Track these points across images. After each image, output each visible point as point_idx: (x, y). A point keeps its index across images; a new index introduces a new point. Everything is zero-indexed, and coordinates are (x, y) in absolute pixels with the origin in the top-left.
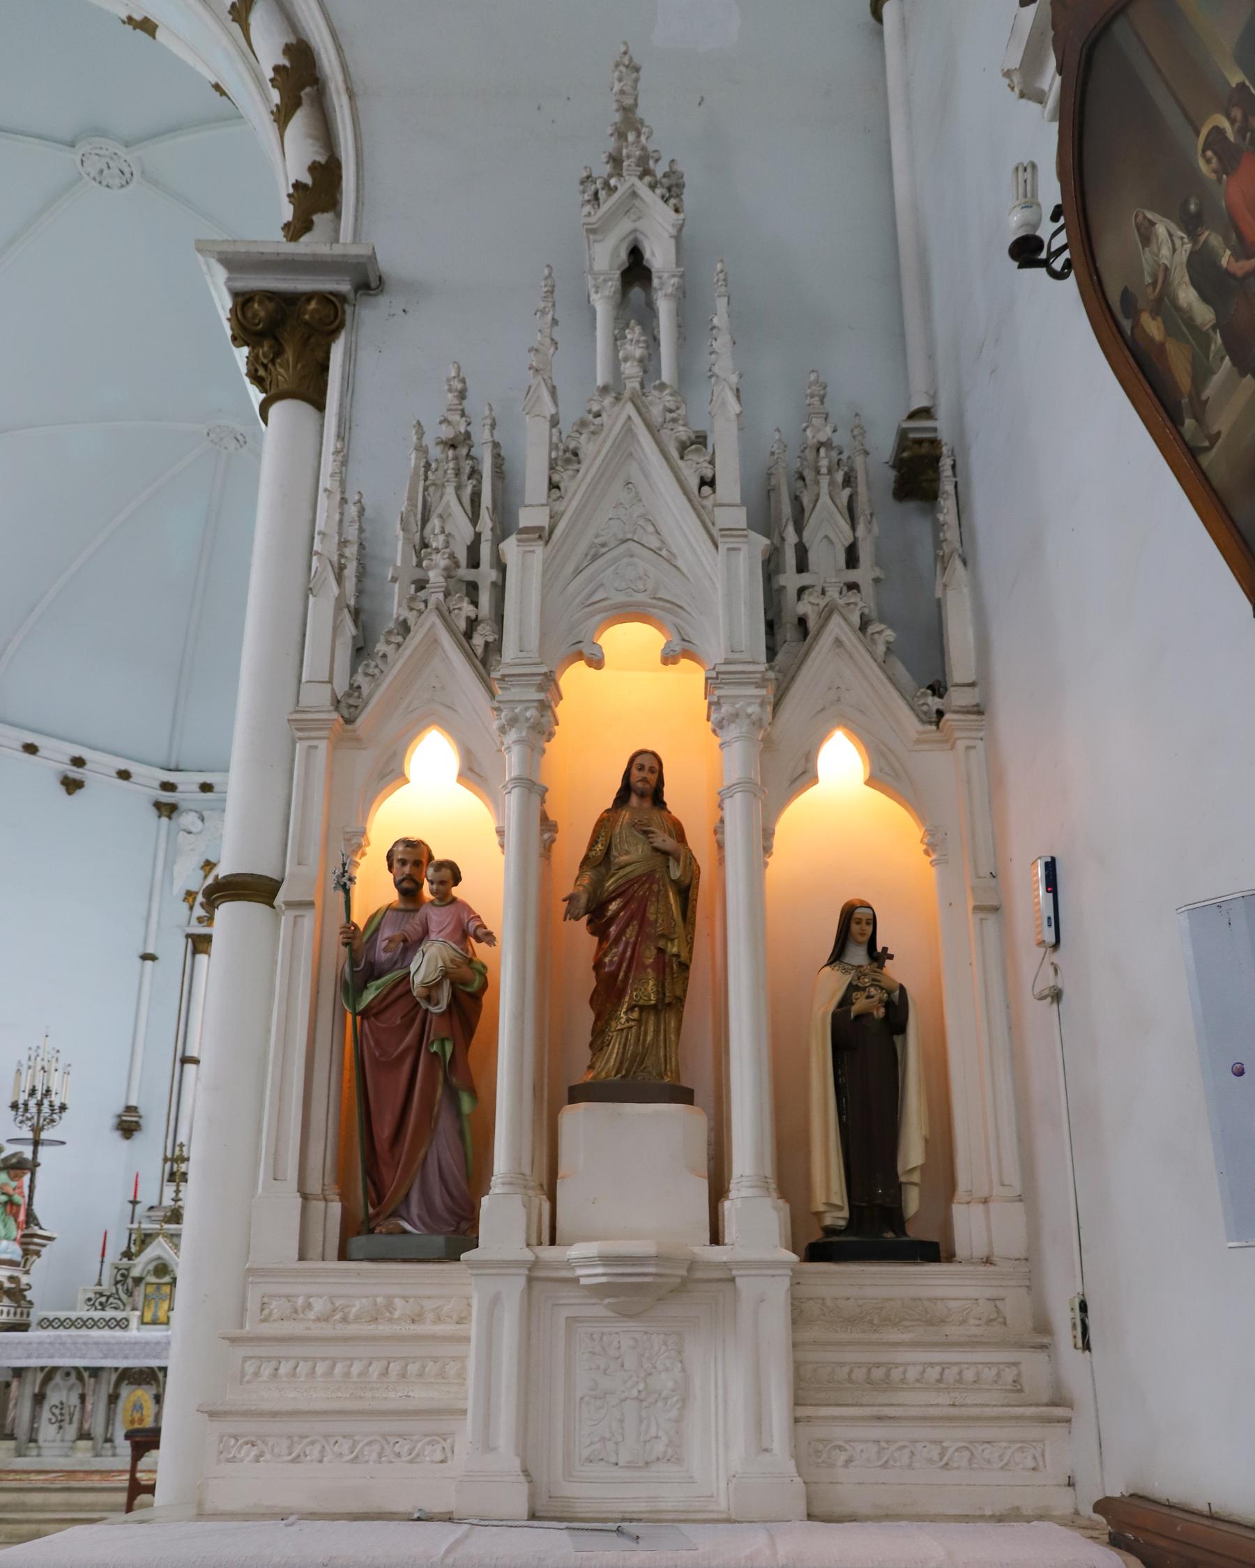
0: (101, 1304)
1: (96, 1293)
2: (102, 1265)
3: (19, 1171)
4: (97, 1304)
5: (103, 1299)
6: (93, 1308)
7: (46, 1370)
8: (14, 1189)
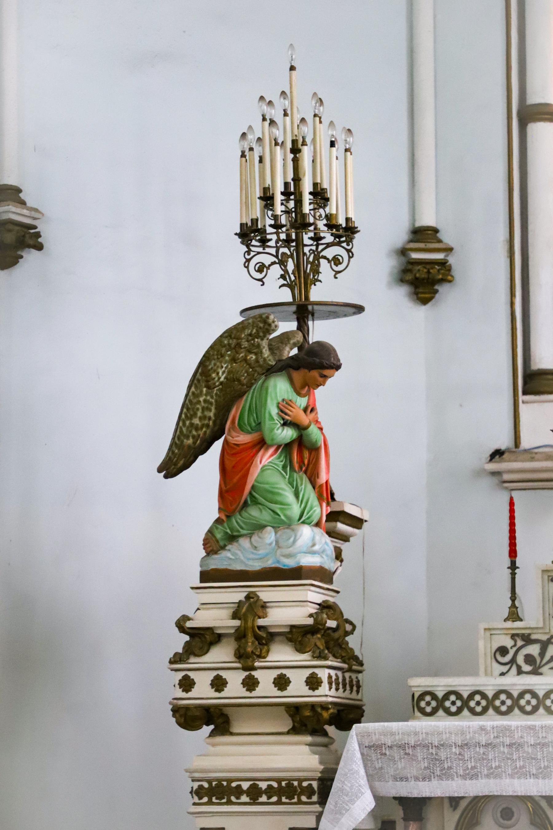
0: (529, 659)
1: (513, 636)
2: (513, 575)
3: (315, 373)
4: (520, 659)
5: (534, 650)
6: (514, 669)
7: (463, 804)
8: (305, 410)
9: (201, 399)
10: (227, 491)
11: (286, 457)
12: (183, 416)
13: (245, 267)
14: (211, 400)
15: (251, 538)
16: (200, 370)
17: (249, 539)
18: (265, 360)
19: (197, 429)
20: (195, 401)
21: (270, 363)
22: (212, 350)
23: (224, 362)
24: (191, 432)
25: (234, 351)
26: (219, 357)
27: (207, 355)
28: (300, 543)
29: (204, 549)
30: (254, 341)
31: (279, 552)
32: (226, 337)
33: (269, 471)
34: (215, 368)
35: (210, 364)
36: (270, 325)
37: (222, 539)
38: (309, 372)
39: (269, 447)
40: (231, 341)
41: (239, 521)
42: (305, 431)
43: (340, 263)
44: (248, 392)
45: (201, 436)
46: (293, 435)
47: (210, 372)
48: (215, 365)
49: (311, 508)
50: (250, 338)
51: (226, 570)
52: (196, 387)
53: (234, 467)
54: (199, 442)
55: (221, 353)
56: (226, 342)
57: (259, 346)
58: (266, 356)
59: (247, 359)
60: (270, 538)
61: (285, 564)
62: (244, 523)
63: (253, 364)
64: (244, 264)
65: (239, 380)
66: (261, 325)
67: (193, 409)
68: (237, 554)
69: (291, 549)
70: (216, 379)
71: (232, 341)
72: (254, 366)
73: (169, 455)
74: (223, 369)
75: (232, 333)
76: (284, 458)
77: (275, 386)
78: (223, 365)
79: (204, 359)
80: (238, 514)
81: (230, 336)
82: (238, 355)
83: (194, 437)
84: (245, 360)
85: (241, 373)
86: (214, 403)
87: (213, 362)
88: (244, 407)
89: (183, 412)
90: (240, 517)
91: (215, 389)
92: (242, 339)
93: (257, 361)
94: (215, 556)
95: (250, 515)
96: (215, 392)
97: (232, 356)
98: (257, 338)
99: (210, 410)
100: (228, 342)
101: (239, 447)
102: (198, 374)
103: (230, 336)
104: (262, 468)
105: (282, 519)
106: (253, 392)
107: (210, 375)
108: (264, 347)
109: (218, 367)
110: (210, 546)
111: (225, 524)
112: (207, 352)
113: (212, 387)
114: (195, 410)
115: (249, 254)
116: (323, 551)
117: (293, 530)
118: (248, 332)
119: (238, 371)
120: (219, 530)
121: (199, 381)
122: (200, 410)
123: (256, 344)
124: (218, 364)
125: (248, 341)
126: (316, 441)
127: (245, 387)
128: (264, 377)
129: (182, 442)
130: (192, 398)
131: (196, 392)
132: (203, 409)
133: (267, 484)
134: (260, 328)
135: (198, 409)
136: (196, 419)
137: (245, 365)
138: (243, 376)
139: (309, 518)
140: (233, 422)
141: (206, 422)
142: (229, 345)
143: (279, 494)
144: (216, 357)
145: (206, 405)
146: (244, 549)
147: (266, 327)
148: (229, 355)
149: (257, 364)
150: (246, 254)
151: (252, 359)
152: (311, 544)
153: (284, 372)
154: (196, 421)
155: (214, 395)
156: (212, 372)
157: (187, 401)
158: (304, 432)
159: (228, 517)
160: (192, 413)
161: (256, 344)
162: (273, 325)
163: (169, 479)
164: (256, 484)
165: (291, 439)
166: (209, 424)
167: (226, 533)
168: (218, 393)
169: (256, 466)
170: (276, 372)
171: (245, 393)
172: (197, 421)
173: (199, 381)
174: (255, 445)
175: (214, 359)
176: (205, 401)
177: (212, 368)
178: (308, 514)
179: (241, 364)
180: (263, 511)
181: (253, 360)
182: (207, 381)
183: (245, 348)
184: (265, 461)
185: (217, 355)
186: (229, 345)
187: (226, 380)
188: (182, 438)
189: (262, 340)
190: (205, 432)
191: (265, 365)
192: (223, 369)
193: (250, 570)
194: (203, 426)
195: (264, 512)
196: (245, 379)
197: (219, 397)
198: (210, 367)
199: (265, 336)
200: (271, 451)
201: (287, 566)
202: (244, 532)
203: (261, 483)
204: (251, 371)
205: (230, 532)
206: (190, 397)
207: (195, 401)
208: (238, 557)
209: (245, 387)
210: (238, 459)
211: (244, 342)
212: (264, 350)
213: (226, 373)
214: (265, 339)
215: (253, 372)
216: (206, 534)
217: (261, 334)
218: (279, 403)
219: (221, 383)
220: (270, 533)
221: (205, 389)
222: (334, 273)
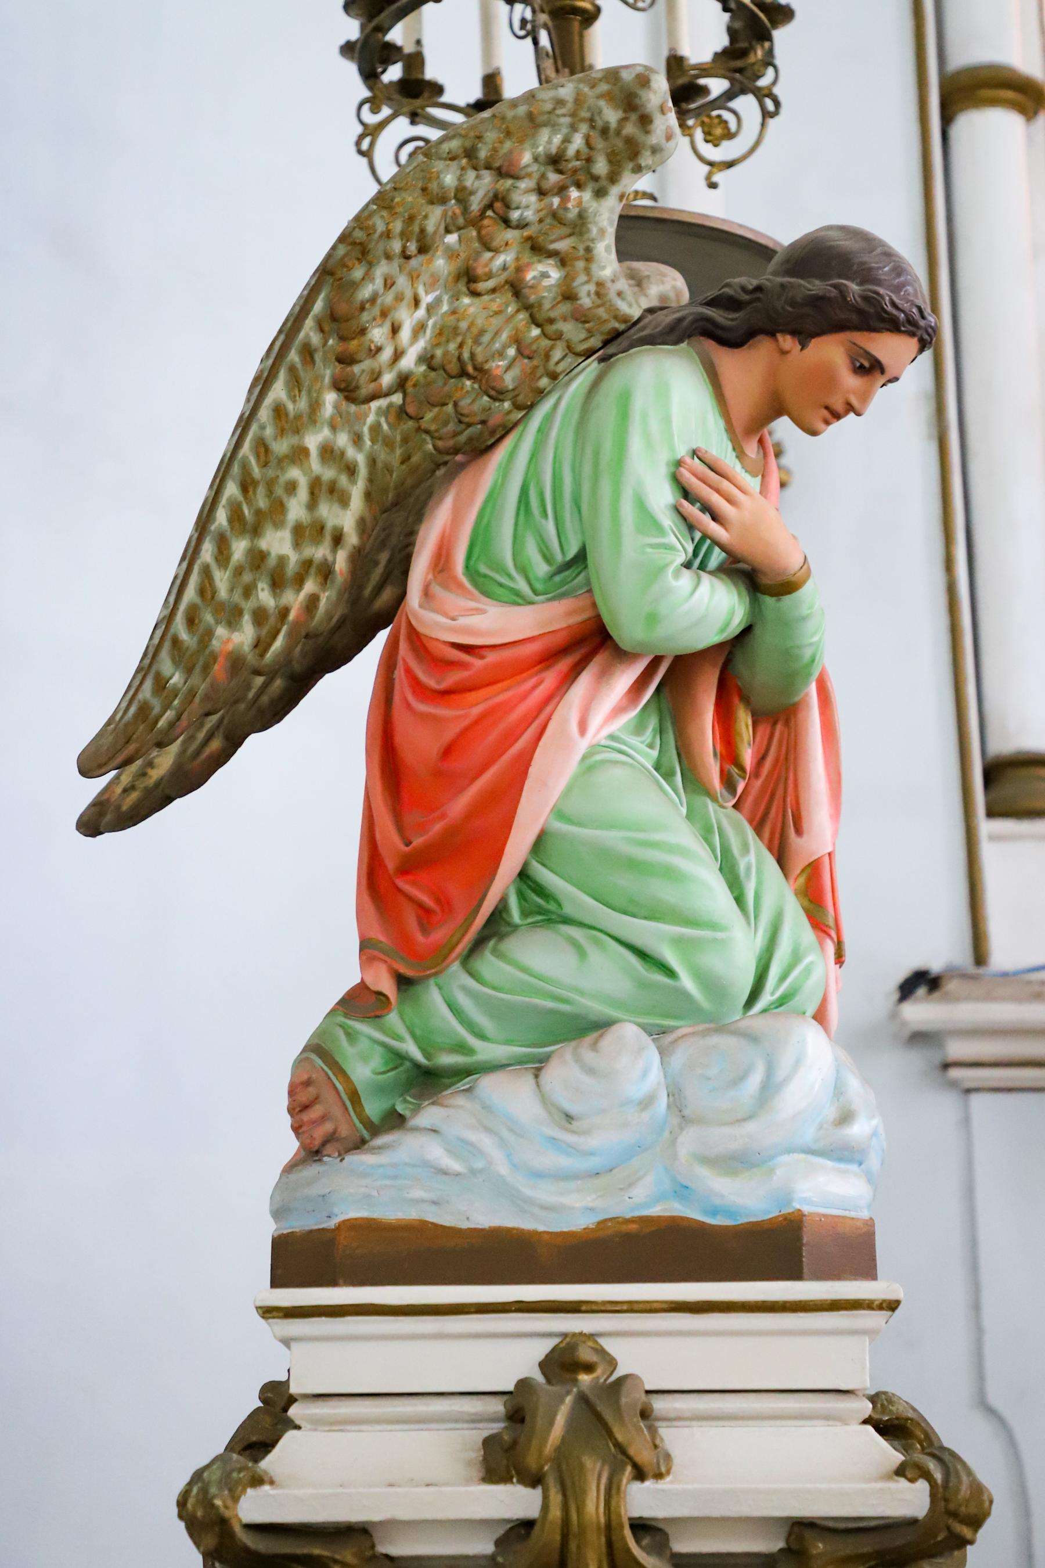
9: (313, 441)
10: (409, 866)
11: (662, 731)
12: (221, 517)
13: (361, 152)
14: (351, 453)
15: (537, 1076)
16: (318, 306)
17: (530, 1078)
19: (277, 584)
22: (385, 213)
23: (425, 277)
25: (474, 233)
26: (412, 247)
27: (359, 235)
29: (297, 1129)
30: (565, 200)
31: (688, 1141)
33: (617, 772)
34: (388, 298)
35: (367, 277)
36: (645, 121)
37: (381, 1090)
38: (803, 346)
39: (622, 655)
41: (464, 1002)
42: (787, 599)
43: (729, 135)
44: (520, 428)
45: (292, 616)
47: (365, 316)
48: (389, 283)
49: (796, 958)
50: (553, 178)
51: (421, 1229)
52: (295, 383)
53: (448, 751)
54: (279, 643)
55: (422, 231)
56: (449, 179)
57: (579, 226)
60: (645, 1074)
61: (717, 1201)
62: (497, 1011)
63: (547, 305)
64: (358, 143)
65: (480, 373)
66: (611, 116)
67: (270, 485)
68: (475, 1150)
69: (751, 1127)
70: (387, 354)
71: (478, 177)
72: (553, 314)
73: (140, 696)
74: (421, 312)
75: (479, 138)
76: (654, 736)
77: (663, 391)
78: (421, 291)
79: (342, 250)
80: (456, 967)
81: (470, 153)
82: (488, 255)
84: (516, 288)
85: (493, 340)
86: (363, 471)
87: (382, 270)
88: (493, 498)
89: (224, 501)
90: (470, 982)
91: (374, 405)
94: (356, 1160)
95: (524, 970)
96: (371, 419)
97: (463, 255)
98: (579, 186)
99: (344, 501)
100: (460, 179)
101: (482, 657)
102: (309, 323)
104: (584, 758)
105: (686, 995)
106: (543, 432)
107: (363, 331)
109: (399, 298)
110: (324, 1118)
111: (393, 1018)
112: (360, 221)
113: (364, 391)
114: (279, 491)
115: (375, 110)
117: (752, 1038)
118: (550, 142)
119: (482, 332)
120: (364, 1044)
121: (308, 353)
122: (303, 493)
123: (572, 214)
127: (507, 405)
128: (595, 364)
130: (269, 432)
131: (290, 406)
133: (610, 825)
134: (605, 131)
135: (291, 487)
136: (279, 534)
137: (510, 309)
138: (501, 354)
140: (441, 562)
141: (320, 552)
142: (462, 195)
143: (670, 874)
144: (396, 246)
145: (328, 474)
146: (515, 1128)
147: (630, 129)
149: (565, 308)
150: (366, 107)
151: (546, 282)
152: (831, 1113)
153: (684, 345)
155: (366, 430)
156: (374, 319)
157: (246, 449)
159: (403, 982)
160: (262, 502)
163: (108, 839)
164: (558, 826)
165: (722, 630)
166: (334, 562)
167: (398, 1057)
168: (385, 427)
170: (651, 341)
171: (507, 430)
172: (282, 539)
173: (308, 353)
174: (548, 658)
175: (388, 257)
176: (328, 453)
177: (373, 299)
178: (783, 978)
179: (493, 300)
180: (595, 956)
181: (548, 288)
182: (346, 360)
183: (522, 225)
184: (600, 727)
185: (404, 236)
186: (462, 195)
187: (423, 368)
188: (208, 618)
189: (600, 193)
190: (313, 601)
191: (601, 312)
195: (595, 956)
196: (508, 368)
197: (389, 443)
198: (365, 292)
199: (613, 178)
201: (727, 1212)
202: (486, 1051)
203: (580, 824)
204: (537, 338)
205: (418, 1056)
206: (263, 428)
207: (281, 447)
208: (479, 1164)
209: (507, 405)
210: (476, 711)
211: (528, 191)
213: (429, 331)
215: (545, 343)
216: (300, 1062)
217: (601, 167)
220: (641, 1050)
221: (330, 398)
222: (706, 168)
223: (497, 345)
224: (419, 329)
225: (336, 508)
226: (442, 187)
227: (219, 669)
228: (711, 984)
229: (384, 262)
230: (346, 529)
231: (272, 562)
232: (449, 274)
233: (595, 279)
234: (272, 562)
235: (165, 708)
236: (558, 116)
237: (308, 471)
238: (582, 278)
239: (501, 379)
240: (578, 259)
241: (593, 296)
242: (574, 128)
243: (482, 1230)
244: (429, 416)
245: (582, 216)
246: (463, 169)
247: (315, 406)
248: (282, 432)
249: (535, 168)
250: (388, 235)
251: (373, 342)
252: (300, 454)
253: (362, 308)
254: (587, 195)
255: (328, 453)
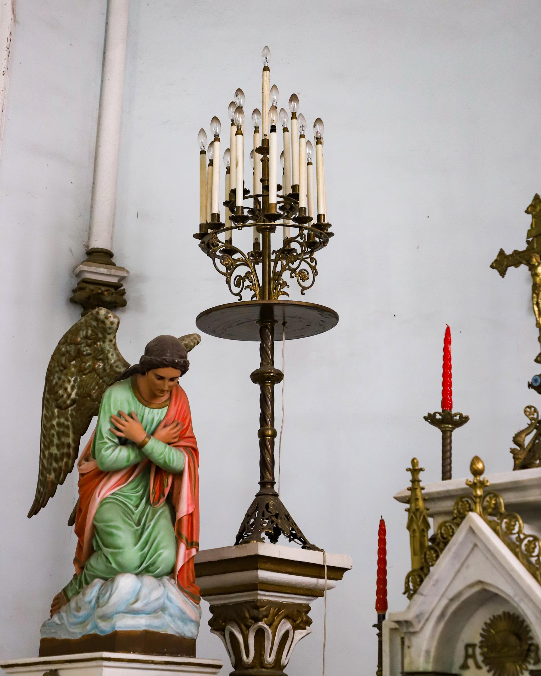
9: (54, 423)
14: (66, 423)
18: (111, 366)
19: (57, 461)
20: (48, 425)
21: (118, 370)
23: (69, 374)
24: (51, 464)
25: (79, 359)
26: (62, 368)
28: (114, 599)
30: (97, 345)
32: (63, 344)
35: (54, 378)
36: (103, 322)
40: (68, 348)
45: (63, 468)
46: (129, 456)
47: (56, 388)
48: (60, 379)
49: (156, 551)
50: (89, 342)
55: (62, 364)
57: (102, 351)
58: (113, 361)
59: (95, 368)
66: (94, 323)
70: (65, 396)
71: (70, 347)
74: (72, 383)
75: (67, 337)
78: (70, 378)
82: (84, 364)
83: (55, 470)
85: (91, 386)
86: (71, 427)
87: (56, 376)
91: (70, 409)
92: (80, 343)
93: (104, 369)
96: (70, 412)
98: (99, 342)
99: (68, 436)
100: (66, 348)
103: (66, 341)
104: (101, 502)
105: (113, 568)
107: (57, 392)
108: (109, 351)
109: (64, 381)
113: (65, 406)
116: (163, 609)
118: (83, 334)
119: (88, 384)
122: (56, 436)
123: (100, 349)
124: (63, 377)
125: (89, 346)
126: (165, 462)
129: (46, 477)
132: (58, 434)
135: (53, 435)
137: (95, 376)
138: (94, 389)
139: (153, 564)
141: (65, 450)
143: (111, 534)
144: (57, 369)
145: (61, 430)
148: (75, 366)
152: (133, 600)
154: (54, 450)
155: (69, 416)
156: (59, 388)
158: (143, 450)
161: (100, 349)
162: (108, 322)
165: (128, 460)
166: (70, 452)
168: (74, 413)
169: (95, 499)
175: (57, 372)
176: (59, 424)
177: (56, 383)
182: (57, 400)
187: (78, 397)
188: (45, 472)
189: (104, 342)
191: (112, 373)
192: (72, 383)
193: (73, 639)
194: (63, 455)
196: (95, 393)
198: (54, 382)
199: (105, 337)
200: (115, 479)
207: (48, 425)
211: (85, 347)
212: (110, 355)
213: (76, 387)
214: (107, 340)
217: (100, 335)
218: (111, 417)
219: (74, 401)
221: (56, 410)
223: (92, 387)
224: (73, 388)
225: (66, 438)
226: (62, 352)
227: (50, 485)
228: (118, 564)
229: (56, 374)
230: (70, 443)
231: (54, 455)
232: (77, 371)
233: (110, 364)
234: (54, 455)
235: (41, 498)
236: (82, 327)
237: (55, 430)
238: (107, 365)
239: (93, 396)
240: (105, 359)
241: (110, 369)
242: (88, 329)
243: (78, 640)
244: (82, 409)
245: (102, 348)
246: (66, 346)
247: (53, 413)
248: (47, 422)
249: (83, 341)
250: (54, 367)
251: (60, 394)
252: (53, 426)
253: (54, 387)
254: (102, 343)
255: (59, 424)
